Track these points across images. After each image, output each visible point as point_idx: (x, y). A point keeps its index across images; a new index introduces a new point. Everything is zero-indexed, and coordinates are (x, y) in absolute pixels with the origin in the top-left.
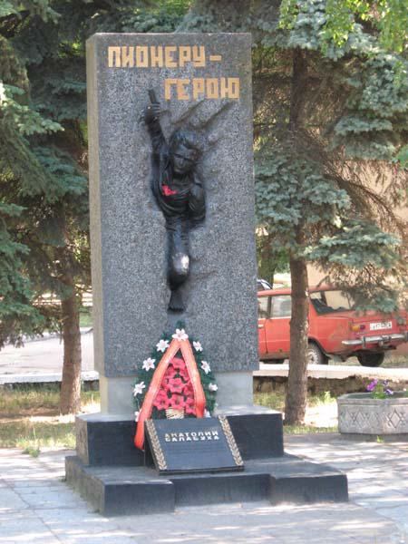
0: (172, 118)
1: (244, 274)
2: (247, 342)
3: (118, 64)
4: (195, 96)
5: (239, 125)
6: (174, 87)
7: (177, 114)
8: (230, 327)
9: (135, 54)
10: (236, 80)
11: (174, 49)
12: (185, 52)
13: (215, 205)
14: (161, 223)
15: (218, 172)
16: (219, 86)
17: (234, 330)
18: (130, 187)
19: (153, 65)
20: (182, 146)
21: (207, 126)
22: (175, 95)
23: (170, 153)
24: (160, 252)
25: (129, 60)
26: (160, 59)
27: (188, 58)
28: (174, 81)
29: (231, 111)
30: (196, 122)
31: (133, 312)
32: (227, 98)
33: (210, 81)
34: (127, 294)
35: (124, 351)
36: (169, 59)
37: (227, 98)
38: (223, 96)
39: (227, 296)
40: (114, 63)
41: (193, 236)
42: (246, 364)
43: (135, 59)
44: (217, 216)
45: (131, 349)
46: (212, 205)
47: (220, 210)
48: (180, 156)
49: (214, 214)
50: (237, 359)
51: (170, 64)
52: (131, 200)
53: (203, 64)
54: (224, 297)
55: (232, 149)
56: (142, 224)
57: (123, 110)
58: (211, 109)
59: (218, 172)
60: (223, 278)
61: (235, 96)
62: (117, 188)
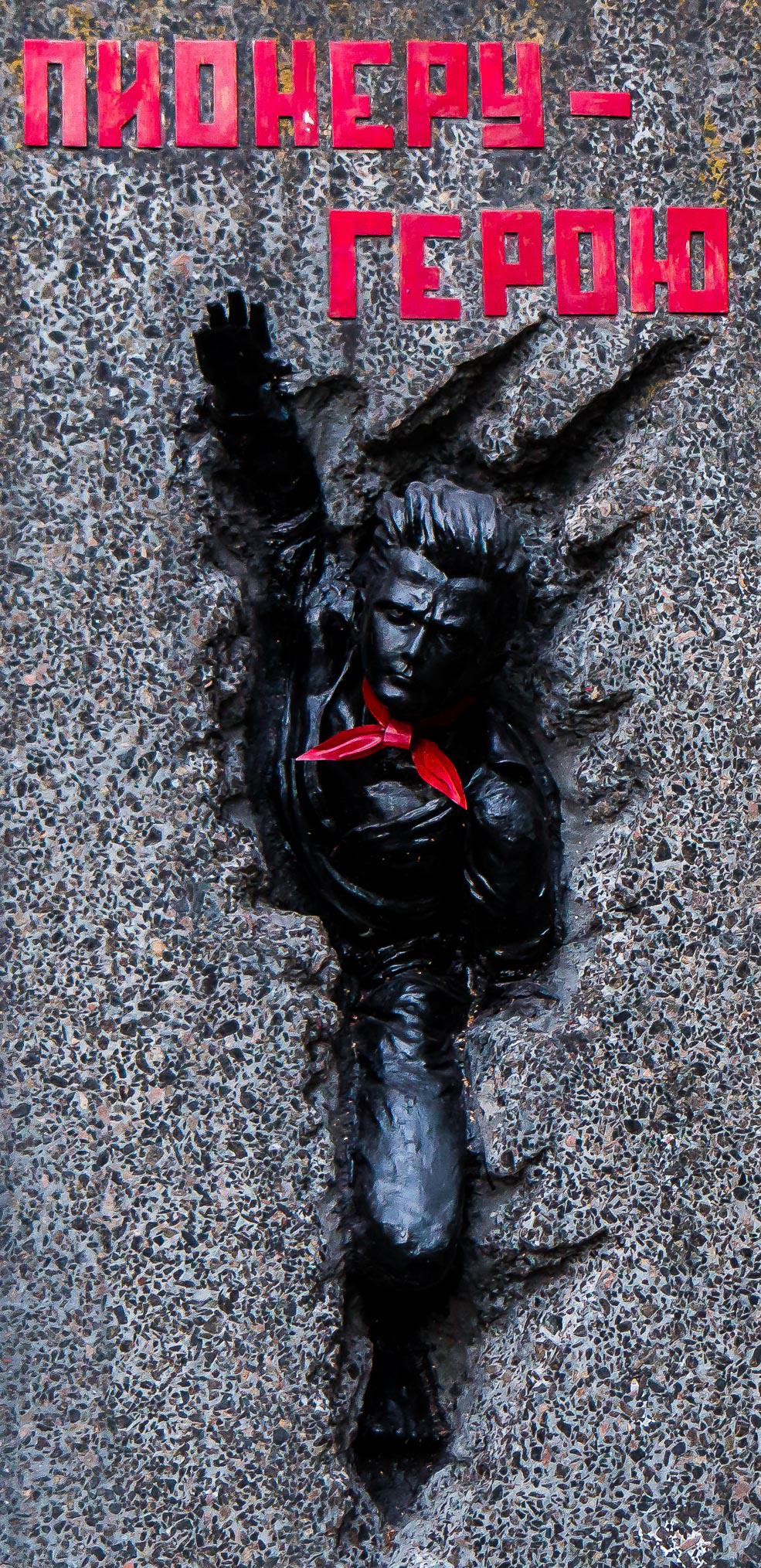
0: (368, 420)
5: (727, 455)
14: (311, 980)
15: (617, 703)
18: (140, 788)
21: (558, 460)
23: (359, 607)
29: (683, 382)
31: (157, 1466)
34: (126, 1369)
39: (673, 1373)
41: (483, 1043)
44: (617, 937)
47: (632, 909)
49: (596, 927)
52: (148, 855)
55: (690, 579)
56: (210, 985)
57: (103, 372)
59: (617, 703)
60: (645, 1275)
62: (72, 794)
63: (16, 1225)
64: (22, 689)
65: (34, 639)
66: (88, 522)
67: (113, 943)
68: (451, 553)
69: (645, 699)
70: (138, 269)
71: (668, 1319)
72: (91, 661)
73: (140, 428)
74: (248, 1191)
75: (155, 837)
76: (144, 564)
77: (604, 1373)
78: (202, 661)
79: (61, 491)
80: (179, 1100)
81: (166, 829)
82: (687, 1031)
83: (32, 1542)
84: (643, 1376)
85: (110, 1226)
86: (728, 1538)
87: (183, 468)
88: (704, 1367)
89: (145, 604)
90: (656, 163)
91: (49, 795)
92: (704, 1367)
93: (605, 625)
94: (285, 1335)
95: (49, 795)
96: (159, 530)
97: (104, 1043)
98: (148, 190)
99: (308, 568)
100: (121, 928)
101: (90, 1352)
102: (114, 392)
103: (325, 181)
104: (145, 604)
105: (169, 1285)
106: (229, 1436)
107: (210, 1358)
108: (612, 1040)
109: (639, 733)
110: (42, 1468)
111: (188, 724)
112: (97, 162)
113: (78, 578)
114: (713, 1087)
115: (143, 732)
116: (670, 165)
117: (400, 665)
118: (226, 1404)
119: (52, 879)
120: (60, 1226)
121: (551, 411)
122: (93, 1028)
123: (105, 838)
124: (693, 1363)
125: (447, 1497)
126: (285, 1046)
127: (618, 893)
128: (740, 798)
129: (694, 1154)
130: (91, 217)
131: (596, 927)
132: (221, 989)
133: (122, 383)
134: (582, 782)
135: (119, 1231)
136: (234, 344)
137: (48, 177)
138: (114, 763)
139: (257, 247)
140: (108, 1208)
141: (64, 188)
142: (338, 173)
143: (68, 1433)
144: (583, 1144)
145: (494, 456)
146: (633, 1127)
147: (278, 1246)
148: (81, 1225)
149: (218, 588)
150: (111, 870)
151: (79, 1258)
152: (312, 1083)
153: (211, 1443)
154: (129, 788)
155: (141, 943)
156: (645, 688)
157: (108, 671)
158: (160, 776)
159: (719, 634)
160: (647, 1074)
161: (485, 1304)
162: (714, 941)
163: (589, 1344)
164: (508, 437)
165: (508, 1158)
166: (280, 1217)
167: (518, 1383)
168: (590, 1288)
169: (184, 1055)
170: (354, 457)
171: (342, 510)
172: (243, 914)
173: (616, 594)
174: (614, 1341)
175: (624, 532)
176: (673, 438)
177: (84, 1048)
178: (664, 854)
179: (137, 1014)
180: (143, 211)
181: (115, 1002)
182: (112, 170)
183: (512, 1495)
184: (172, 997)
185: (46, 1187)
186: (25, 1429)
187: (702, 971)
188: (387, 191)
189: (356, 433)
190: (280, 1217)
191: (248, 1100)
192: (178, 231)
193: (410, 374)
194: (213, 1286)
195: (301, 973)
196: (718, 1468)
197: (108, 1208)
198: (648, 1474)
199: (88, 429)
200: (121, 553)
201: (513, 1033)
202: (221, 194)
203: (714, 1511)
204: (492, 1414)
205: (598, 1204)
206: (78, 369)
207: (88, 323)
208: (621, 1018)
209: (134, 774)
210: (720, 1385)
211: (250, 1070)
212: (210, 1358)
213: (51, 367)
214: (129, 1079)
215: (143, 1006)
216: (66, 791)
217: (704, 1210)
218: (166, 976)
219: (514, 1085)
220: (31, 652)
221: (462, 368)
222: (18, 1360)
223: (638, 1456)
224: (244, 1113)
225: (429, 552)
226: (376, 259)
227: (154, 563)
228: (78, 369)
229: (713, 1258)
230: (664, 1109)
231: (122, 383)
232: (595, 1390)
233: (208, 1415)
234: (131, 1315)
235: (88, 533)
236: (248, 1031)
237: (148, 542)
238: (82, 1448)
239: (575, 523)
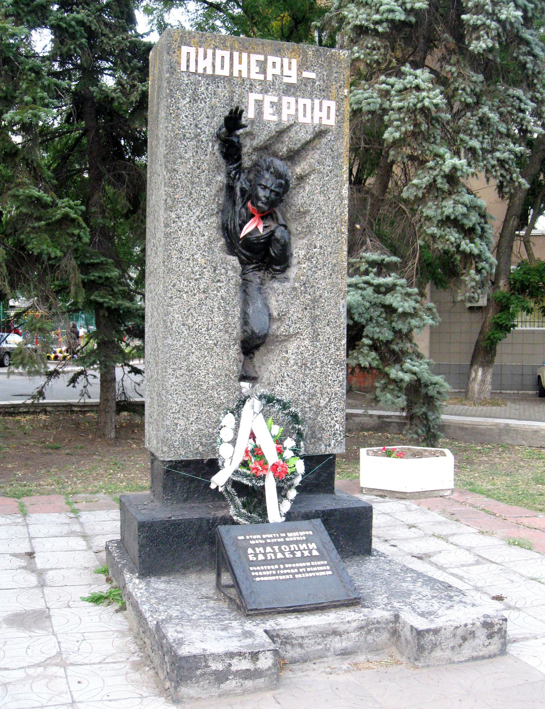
1: (332, 339)
2: (332, 419)
3: (192, 69)
4: (284, 118)
5: (333, 158)
6: (259, 104)
7: (261, 138)
8: (313, 402)
9: (214, 59)
10: (333, 105)
11: (261, 58)
12: (274, 63)
13: (302, 253)
14: (236, 272)
15: (306, 212)
16: (313, 109)
17: (318, 406)
18: (201, 224)
19: (236, 74)
20: (267, 176)
21: (293, 156)
22: (260, 112)
24: (234, 307)
25: (204, 65)
26: (244, 67)
27: (277, 71)
28: (259, 97)
29: (324, 140)
30: (283, 149)
31: (199, 381)
32: (320, 125)
33: (301, 101)
34: (193, 358)
35: (186, 429)
36: (255, 69)
37: (320, 125)
39: (312, 364)
40: (188, 67)
42: (330, 445)
43: (214, 66)
44: (304, 266)
45: (194, 427)
48: (265, 187)
50: (320, 439)
53: (293, 80)
54: (309, 365)
55: (324, 185)
56: (215, 271)
57: (196, 126)
58: (304, 136)
59: (306, 212)
60: (307, 342)
61: (332, 122)
63: (169, 324)
64: (175, 199)
65: (178, 187)
66: (191, 161)
67: (193, 260)
69: (313, 212)
70: (205, 102)
71: (311, 352)
72: (191, 193)
73: (204, 139)
74: (221, 319)
75: (204, 235)
76: (204, 171)
77: (297, 364)
78: (215, 195)
79: (186, 153)
80: (207, 297)
81: (206, 234)
82: (318, 288)
83: (170, 397)
84: (305, 364)
85: (190, 325)
86: (322, 401)
87: (213, 150)
88: (318, 363)
89: (203, 181)
90: (320, 90)
91: (180, 224)
92: (318, 363)
93: (305, 194)
94: (228, 352)
95: (180, 224)
96: (208, 164)
97: (190, 283)
98: (208, 84)
99: (237, 176)
100: (195, 256)
101: (185, 354)
102: (199, 130)
103: (248, 86)
104: (203, 181)
105: (203, 339)
106: (215, 375)
107: (211, 357)
108: (302, 289)
109: (311, 219)
110: (173, 380)
111: (212, 209)
112: (197, 76)
113: (189, 173)
114: (323, 301)
115: (202, 211)
116: (324, 91)
117: (263, 199)
118: (215, 367)
119: (180, 244)
120: (179, 325)
121: (295, 144)
123: (192, 235)
124: (316, 362)
126: (231, 286)
127: (305, 256)
128: (332, 236)
129: (319, 315)
130: (195, 89)
131: (299, 263)
132: (217, 272)
133: (201, 129)
134: (297, 230)
135: (192, 327)
136: (234, 120)
137: (186, 79)
138: (195, 218)
139: (232, 100)
140: (190, 322)
141: (189, 82)
142: (251, 85)
143: (179, 372)
144: (295, 312)
145: (281, 154)
146: (306, 309)
147: (227, 332)
148: (184, 325)
149: (220, 178)
150: (193, 242)
151: (183, 332)
153: (211, 376)
154: (198, 223)
155: (199, 260)
156: (313, 209)
157: (195, 196)
158: (206, 221)
159: (329, 198)
160: (309, 297)
161: (270, 347)
162: (325, 268)
163: (294, 357)
164: (285, 149)
165: (279, 314)
166: (228, 325)
167: (278, 365)
168: (295, 344)
169: (208, 287)
170: (250, 151)
171: (246, 162)
173: (307, 188)
174: (300, 357)
175: (309, 174)
176: (322, 153)
177: (186, 284)
178: (315, 248)
179: (198, 277)
180: (207, 89)
181: (193, 273)
182: (200, 78)
183: (276, 390)
184: (206, 273)
185: (176, 316)
186: (170, 371)
187: (322, 274)
188: (262, 90)
189: (251, 146)
190: (228, 325)
191: (222, 298)
192: (215, 94)
193: (265, 133)
194: (213, 340)
196: (320, 386)
197: (190, 322)
198: (306, 386)
199: (192, 139)
200: (199, 168)
201: (279, 286)
202: (225, 87)
203: (319, 395)
204: (271, 372)
205: (297, 326)
206: (191, 124)
207: (193, 114)
208: (304, 284)
209: (199, 220)
210: (322, 367)
211: (223, 291)
212: (211, 357)
213: (185, 123)
214: (195, 292)
215: (200, 275)
216: (184, 223)
217: (320, 328)
218: (205, 268)
219: (281, 297)
220: (177, 190)
221: (277, 132)
222: (168, 355)
223: (304, 382)
224: (221, 301)
225: (271, 173)
226: (259, 105)
227: (206, 172)
228: (191, 124)
229: (321, 339)
230: (312, 305)
231: (201, 129)
232: (295, 367)
233: (210, 370)
234: (194, 346)
235: (191, 163)
236: (223, 282)
237: (205, 166)
238: (182, 376)
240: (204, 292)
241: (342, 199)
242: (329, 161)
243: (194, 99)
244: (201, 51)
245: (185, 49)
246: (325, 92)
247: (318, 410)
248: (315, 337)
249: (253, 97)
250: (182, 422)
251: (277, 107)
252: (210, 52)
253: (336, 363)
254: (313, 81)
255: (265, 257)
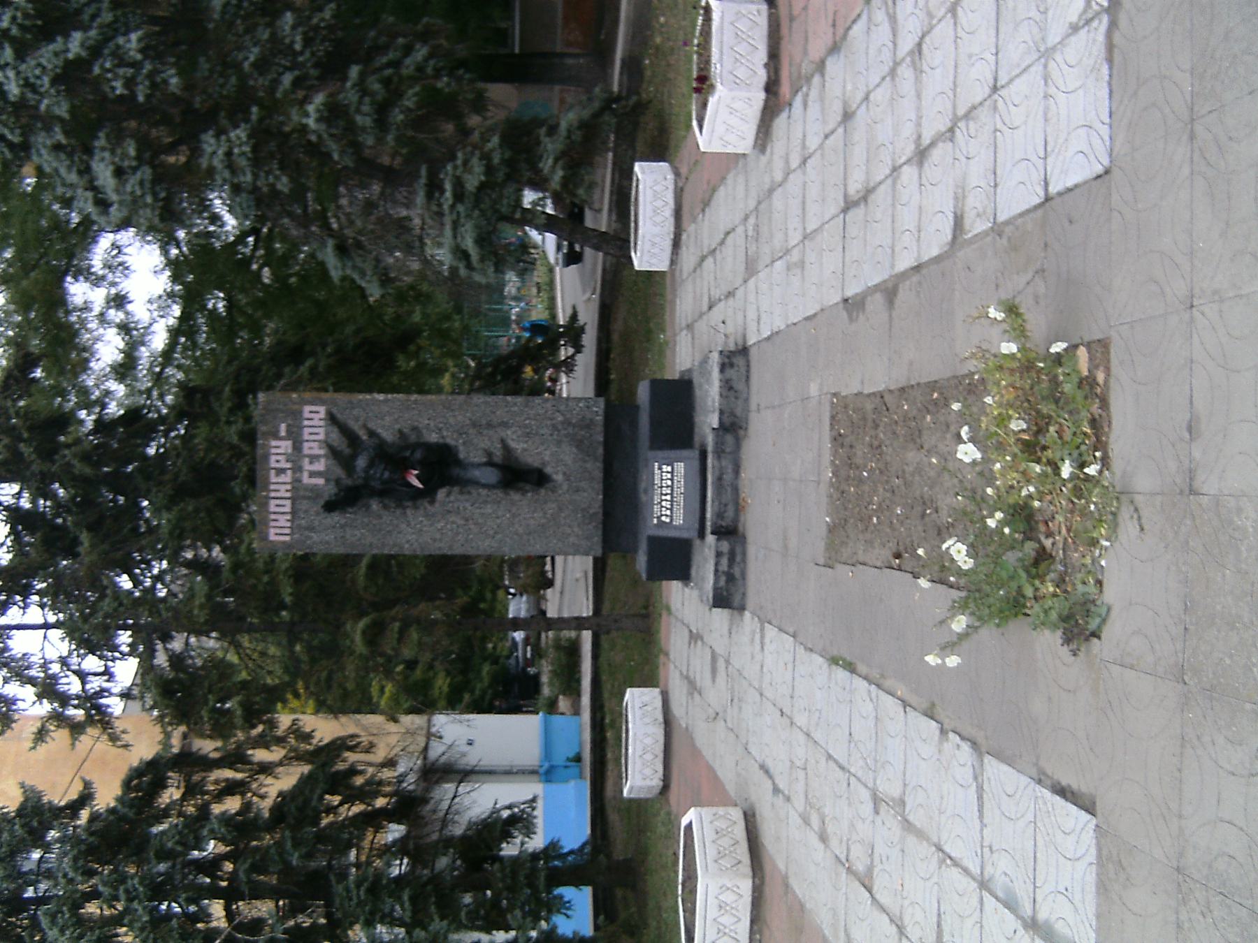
3: (287, 531)
4: (322, 452)
7: (339, 472)
10: (307, 409)
11: (273, 472)
13: (434, 435)
17: (563, 423)
19: (288, 495)
24: (479, 494)
25: (284, 521)
28: (306, 475)
29: (339, 416)
30: (347, 451)
33: (306, 437)
34: (521, 530)
38: (322, 423)
45: (576, 529)
46: (433, 438)
50: (591, 420)
51: (287, 478)
52: (425, 522)
53: (289, 443)
60: (509, 432)
61: (322, 410)
68: (371, 465)
122: (458, 534)
125: (548, 470)
144: (484, 443)
152: (469, 493)
156: (397, 427)
157: (390, 528)
172: (437, 505)
195: (448, 494)
237: (366, 520)
239: (365, 438)
240: (467, 520)
241: (386, 401)
242: (355, 412)
243: (311, 528)
244: (273, 524)
245: (272, 537)
246: (297, 415)
247: (567, 423)
248: (505, 425)
249: (306, 479)
250: (572, 539)
251: (313, 458)
252: (273, 517)
253: (526, 406)
254: (288, 426)
255: (441, 467)
